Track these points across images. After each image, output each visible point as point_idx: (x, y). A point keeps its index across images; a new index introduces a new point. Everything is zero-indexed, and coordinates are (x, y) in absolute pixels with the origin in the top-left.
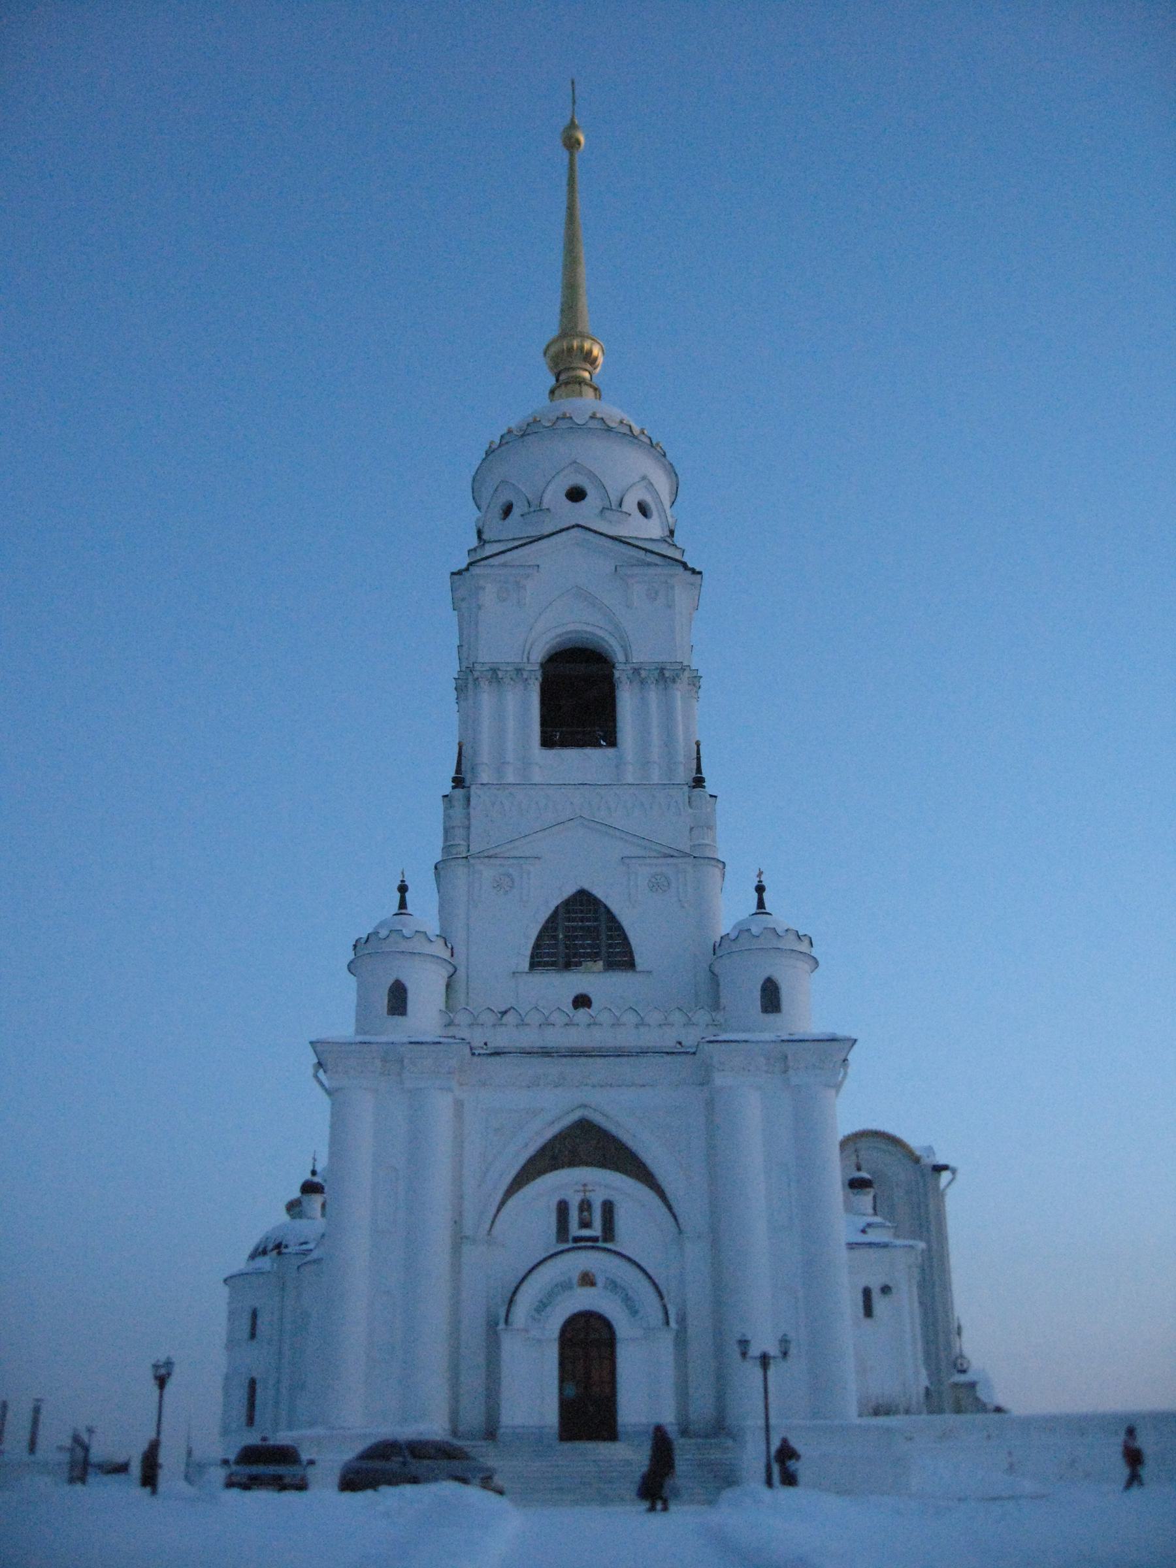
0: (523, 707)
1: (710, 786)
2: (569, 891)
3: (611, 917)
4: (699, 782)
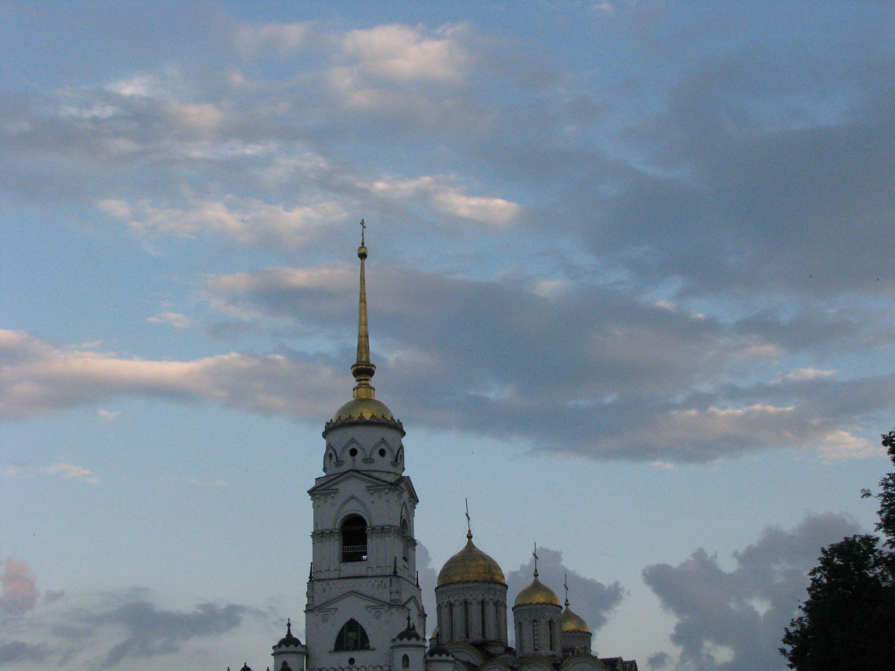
0: (334, 547)
1: (399, 574)
2: (348, 619)
3: (362, 629)
4: (395, 572)
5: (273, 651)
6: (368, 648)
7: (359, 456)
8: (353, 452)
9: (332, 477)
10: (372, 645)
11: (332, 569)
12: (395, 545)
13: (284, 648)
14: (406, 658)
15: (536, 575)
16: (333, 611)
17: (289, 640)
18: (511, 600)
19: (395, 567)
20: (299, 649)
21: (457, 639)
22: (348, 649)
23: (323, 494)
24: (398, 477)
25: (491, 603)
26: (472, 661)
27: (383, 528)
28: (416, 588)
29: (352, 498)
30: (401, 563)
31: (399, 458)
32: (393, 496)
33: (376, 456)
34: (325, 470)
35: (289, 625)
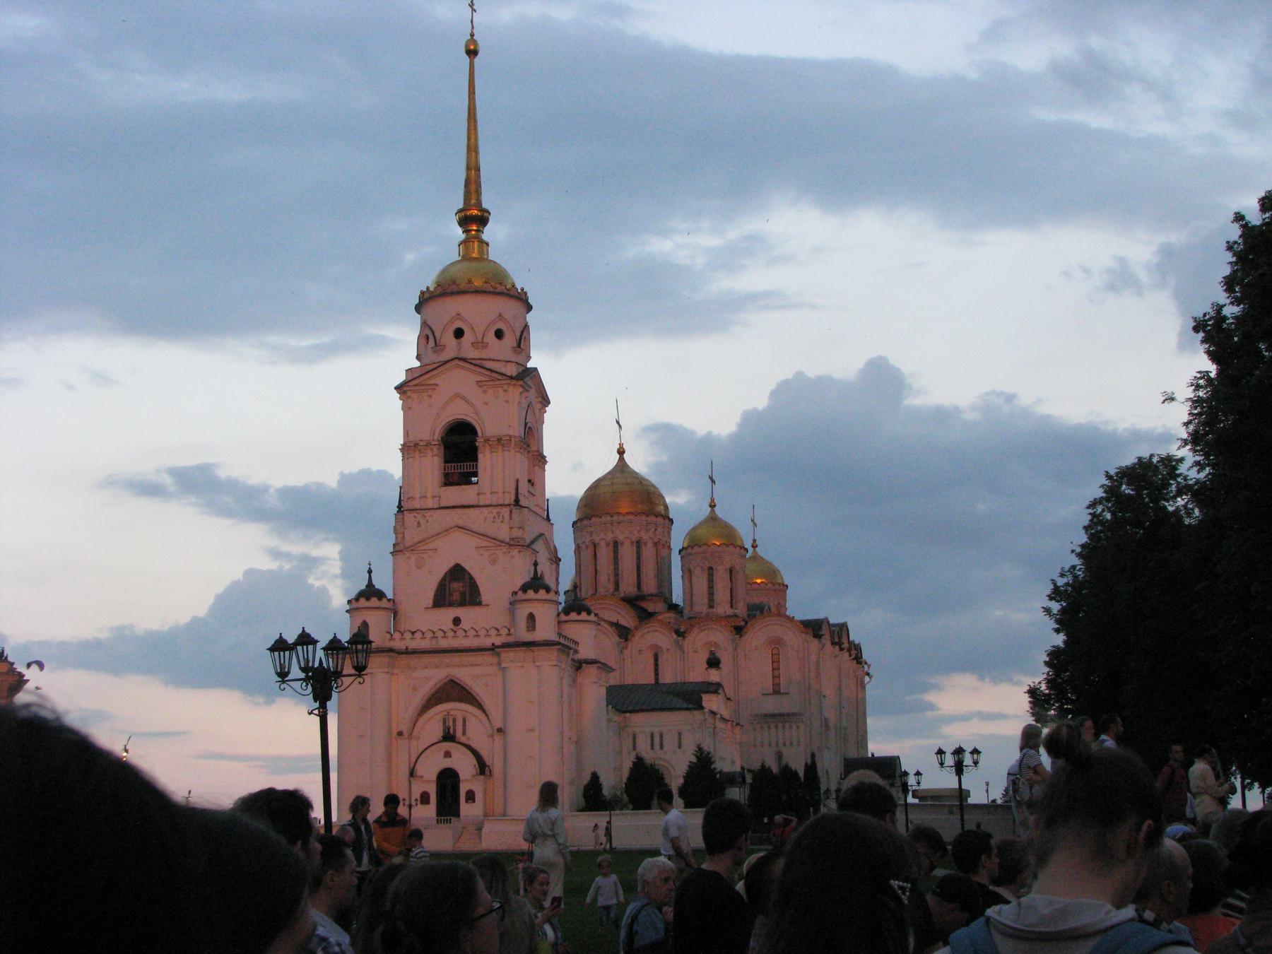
0: (433, 464)
1: (522, 502)
2: (452, 564)
3: (471, 578)
4: (517, 501)
5: (348, 607)
6: (479, 604)
7: (468, 338)
8: (459, 333)
9: (430, 368)
11: (429, 495)
12: (517, 464)
13: (363, 602)
14: (531, 617)
15: (712, 506)
17: (371, 592)
18: (677, 540)
19: (517, 494)
20: (384, 603)
21: (601, 590)
22: (451, 605)
23: (414, 391)
24: (521, 369)
25: (650, 545)
26: (623, 622)
27: (499, 440)
28: (546, 523)
29: (458, 396)
30: (524, 486)
31: (522, 343)
32: (514, 393)
33: (491, 335)
34: (418, 357)
35: (370, 572)
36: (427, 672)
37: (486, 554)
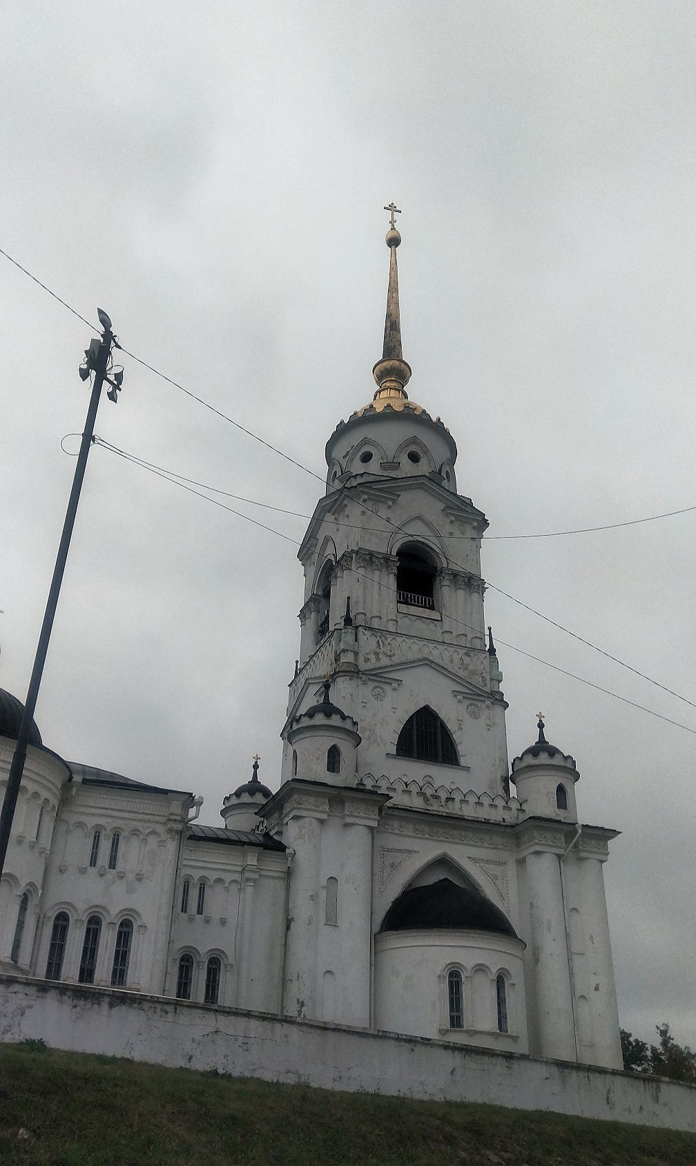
8: (414, 458)
10: (463, 761)
14: (561, 790)
16: (395, 685)
29: (419, 518)
36: (409, 844)
37: (467, 702)
